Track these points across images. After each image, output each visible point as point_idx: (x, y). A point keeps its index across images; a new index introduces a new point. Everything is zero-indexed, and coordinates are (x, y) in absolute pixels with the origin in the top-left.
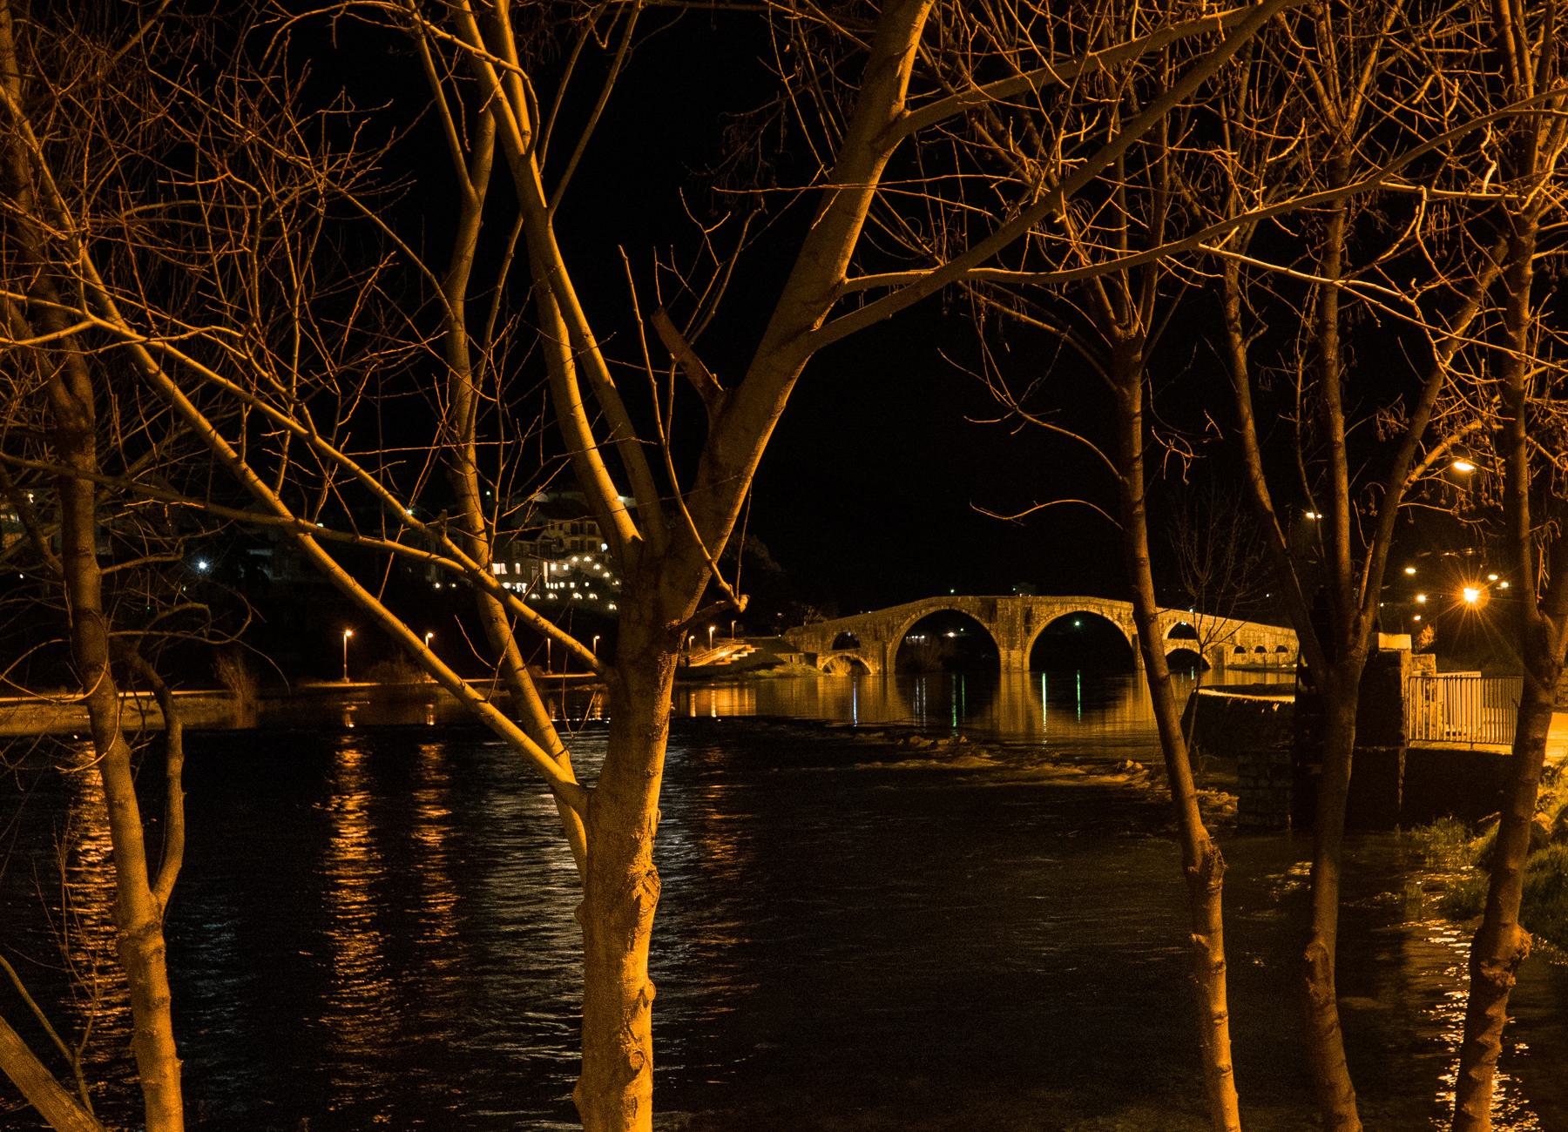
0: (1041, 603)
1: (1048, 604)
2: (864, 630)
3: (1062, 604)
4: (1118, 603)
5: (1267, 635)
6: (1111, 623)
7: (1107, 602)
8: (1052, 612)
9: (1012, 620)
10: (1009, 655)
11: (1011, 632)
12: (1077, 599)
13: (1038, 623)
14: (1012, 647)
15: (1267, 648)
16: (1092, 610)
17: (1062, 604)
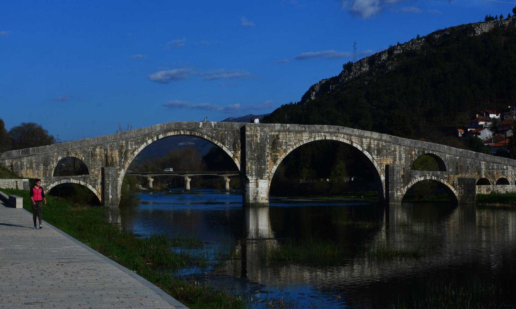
0: (289, 131)
1: (297, 132)
2: (93, 155)
3: (311, 132)
4: (368, 133)
5: (510, 168)
6: (361, 153)
7: (357, 132)
8: (300, 141)
9: (261, 148)
10: (257, 186)
11: (260, 160)
12: (326, 127)
13: (285, 151)
14: (260, 175)
15: (510, 179)
16: (341, 140)
17: (311, 132)
